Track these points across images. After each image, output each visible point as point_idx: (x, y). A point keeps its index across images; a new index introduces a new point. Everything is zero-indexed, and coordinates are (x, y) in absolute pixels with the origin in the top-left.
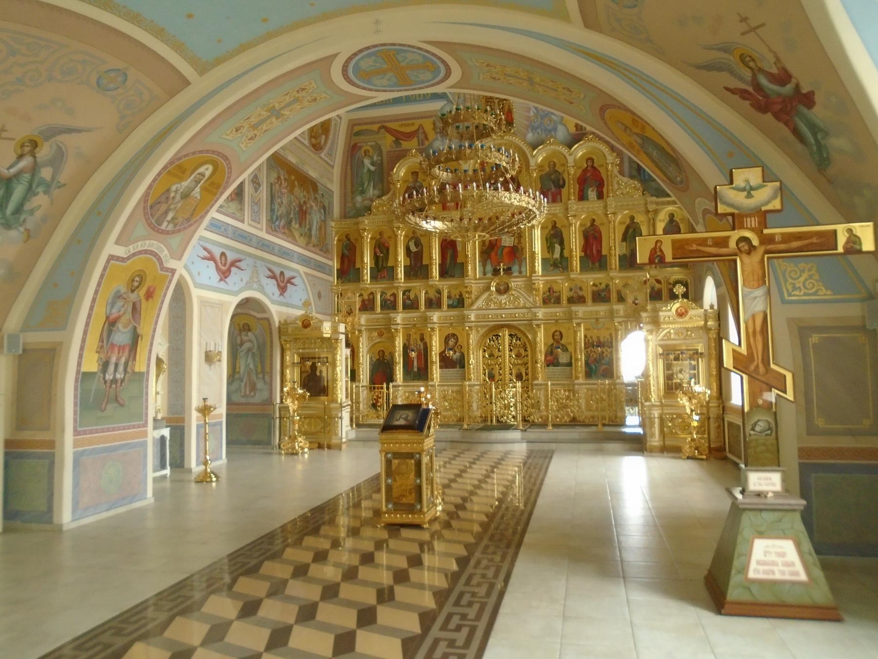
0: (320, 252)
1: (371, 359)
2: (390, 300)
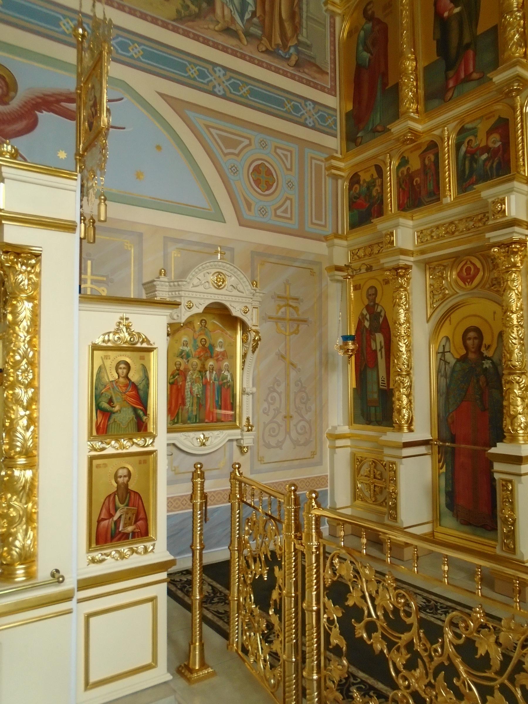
0: (266, 59)
1: (442, 354)
2: (486, 149)
